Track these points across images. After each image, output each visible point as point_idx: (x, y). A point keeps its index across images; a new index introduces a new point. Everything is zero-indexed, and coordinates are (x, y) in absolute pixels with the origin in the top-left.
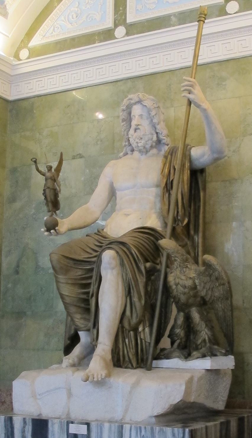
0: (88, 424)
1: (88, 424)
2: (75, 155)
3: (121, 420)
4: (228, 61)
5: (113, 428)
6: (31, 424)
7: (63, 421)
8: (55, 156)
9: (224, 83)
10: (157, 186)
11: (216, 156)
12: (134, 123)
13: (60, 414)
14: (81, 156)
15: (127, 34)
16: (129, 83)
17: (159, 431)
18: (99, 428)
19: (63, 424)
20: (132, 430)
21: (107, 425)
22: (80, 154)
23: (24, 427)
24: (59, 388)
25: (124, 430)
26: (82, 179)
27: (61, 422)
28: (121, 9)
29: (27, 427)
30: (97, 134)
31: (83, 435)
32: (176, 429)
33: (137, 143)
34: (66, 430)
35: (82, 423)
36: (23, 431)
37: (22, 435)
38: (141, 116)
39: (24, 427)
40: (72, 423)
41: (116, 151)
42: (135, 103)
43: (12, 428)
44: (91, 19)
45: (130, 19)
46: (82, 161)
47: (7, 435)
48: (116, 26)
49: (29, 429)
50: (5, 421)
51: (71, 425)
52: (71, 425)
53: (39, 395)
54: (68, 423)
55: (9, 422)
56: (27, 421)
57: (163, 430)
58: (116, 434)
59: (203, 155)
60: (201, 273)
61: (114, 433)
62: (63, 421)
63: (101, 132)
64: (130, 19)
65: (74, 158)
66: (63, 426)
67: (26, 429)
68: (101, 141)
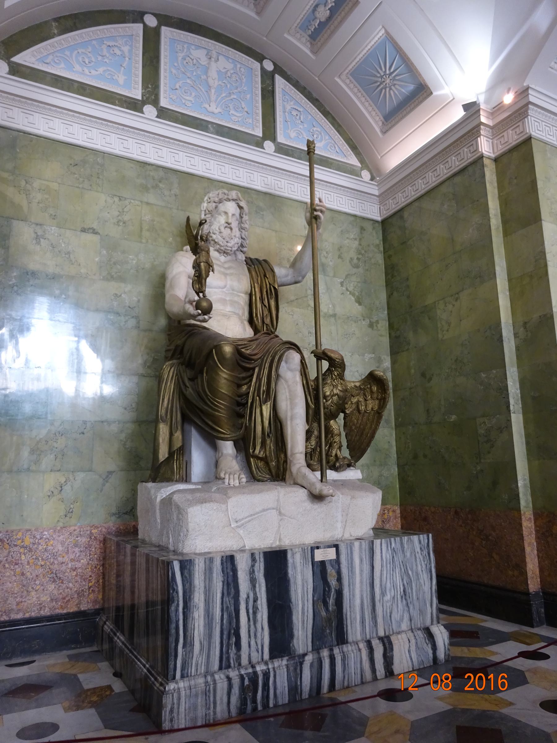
0: (337, 546)
1: (337, 546)
2: (85, 227)
3: (342, 537)
4: (266, 193)
5: (363, 546)
6: (262, 560)
7: (306, 548)
8: (54, 219)
9: (262, 213)
10: (246, 293)
11: (300, 278)
12: (222, 220)
13: (271, 541)
14: (95, 232)
15: (157, 117)
16: (161, 173)
17: (408, 541)
18: (349, 548)
19: (306, 551)
20: (383, 545)
21: (357, 544)
22: (94, 230)
23: (253, 566)
24: (267, 510)
25: (374, 546)
26: (97, 259)
27: (303, 550)
28: (150, 86)
29: (257, 565)
30: (118, 213)
31: (331, 560)
32: (421, 536)
33: (227, 242)
34: (310, 559)
35: (329, 547)
36: (252, 572)
37: (250, 577)
38: (233, 215)
39: (253, 566)
40: (318, 548)
41: (144, 241)
42: (229, 200)
43: (234, 570)
44: (109, 77)
45: (164, 103)
46: (96, 238)
47: (225, 583)
48: (144, 102)
49: (260, 567)
50: (222, 564)
51: (316, 551)
52: (316, 551)
53: (237, 522)
54: (312, 549)
55: (229, 564)
56: (257, 558)
57: (411, 539)
58: (367, 552)
59: (287, 276)
60: (356, 386)
61: (365, 550)
62: (306, 548)
63: (123, 212)
64: (164, 103)
65: (83, 230)
66: (306, 554)
67: (256, 568)
68: (124, 223)
